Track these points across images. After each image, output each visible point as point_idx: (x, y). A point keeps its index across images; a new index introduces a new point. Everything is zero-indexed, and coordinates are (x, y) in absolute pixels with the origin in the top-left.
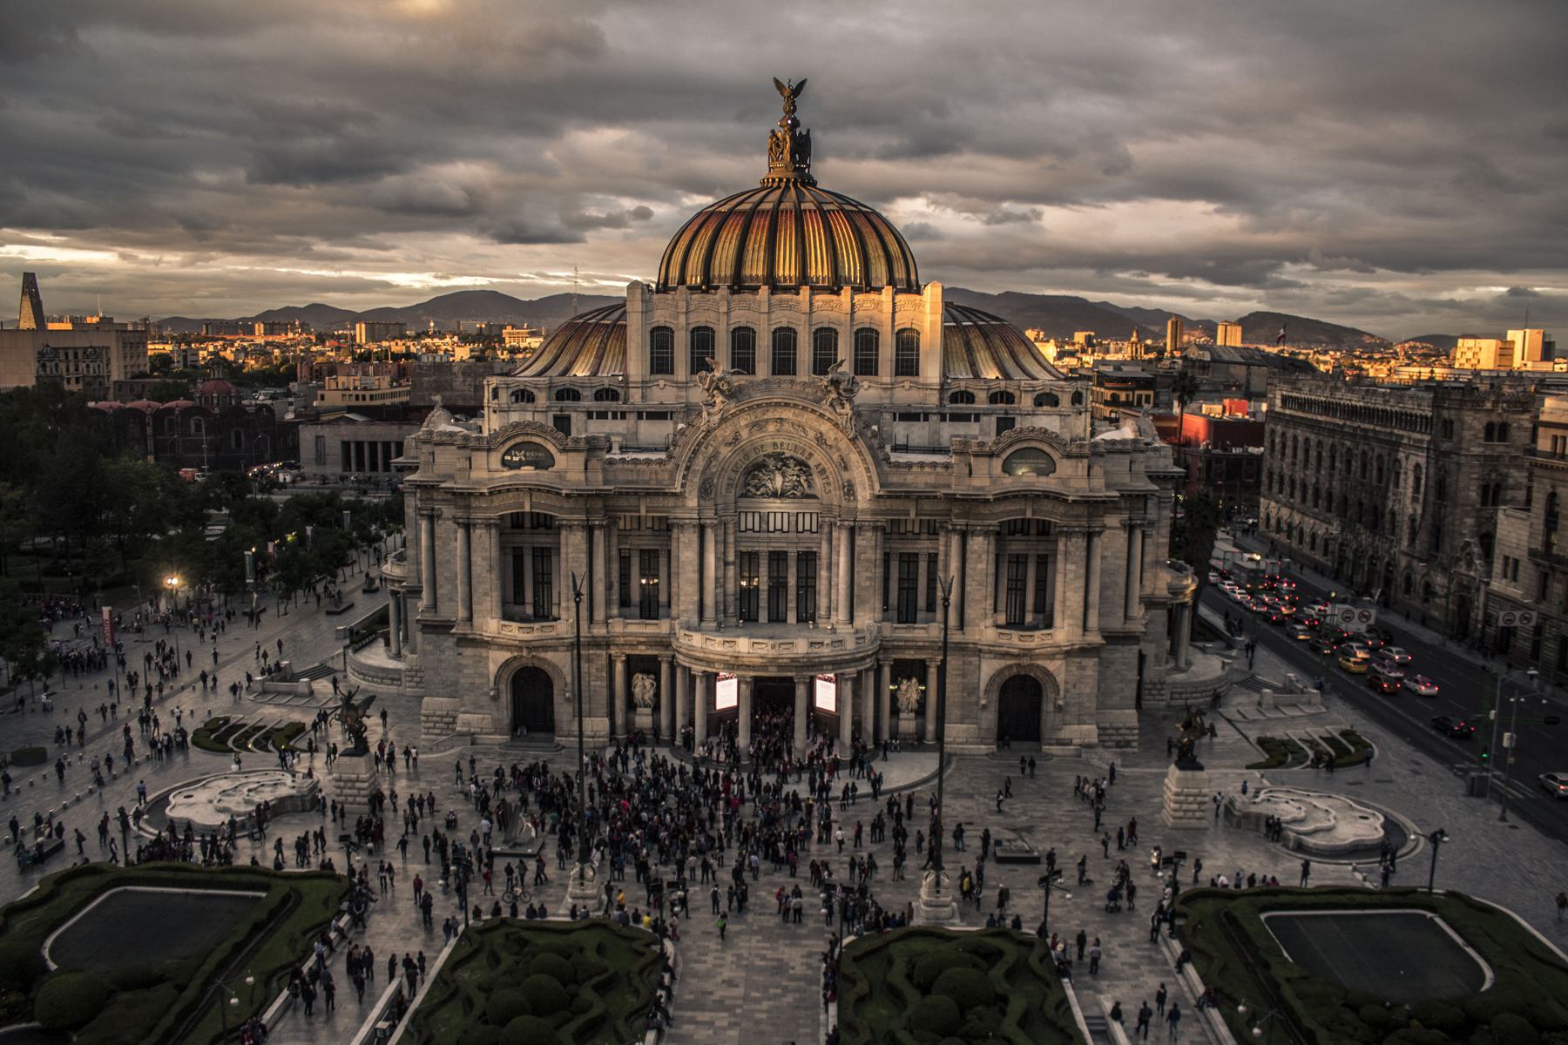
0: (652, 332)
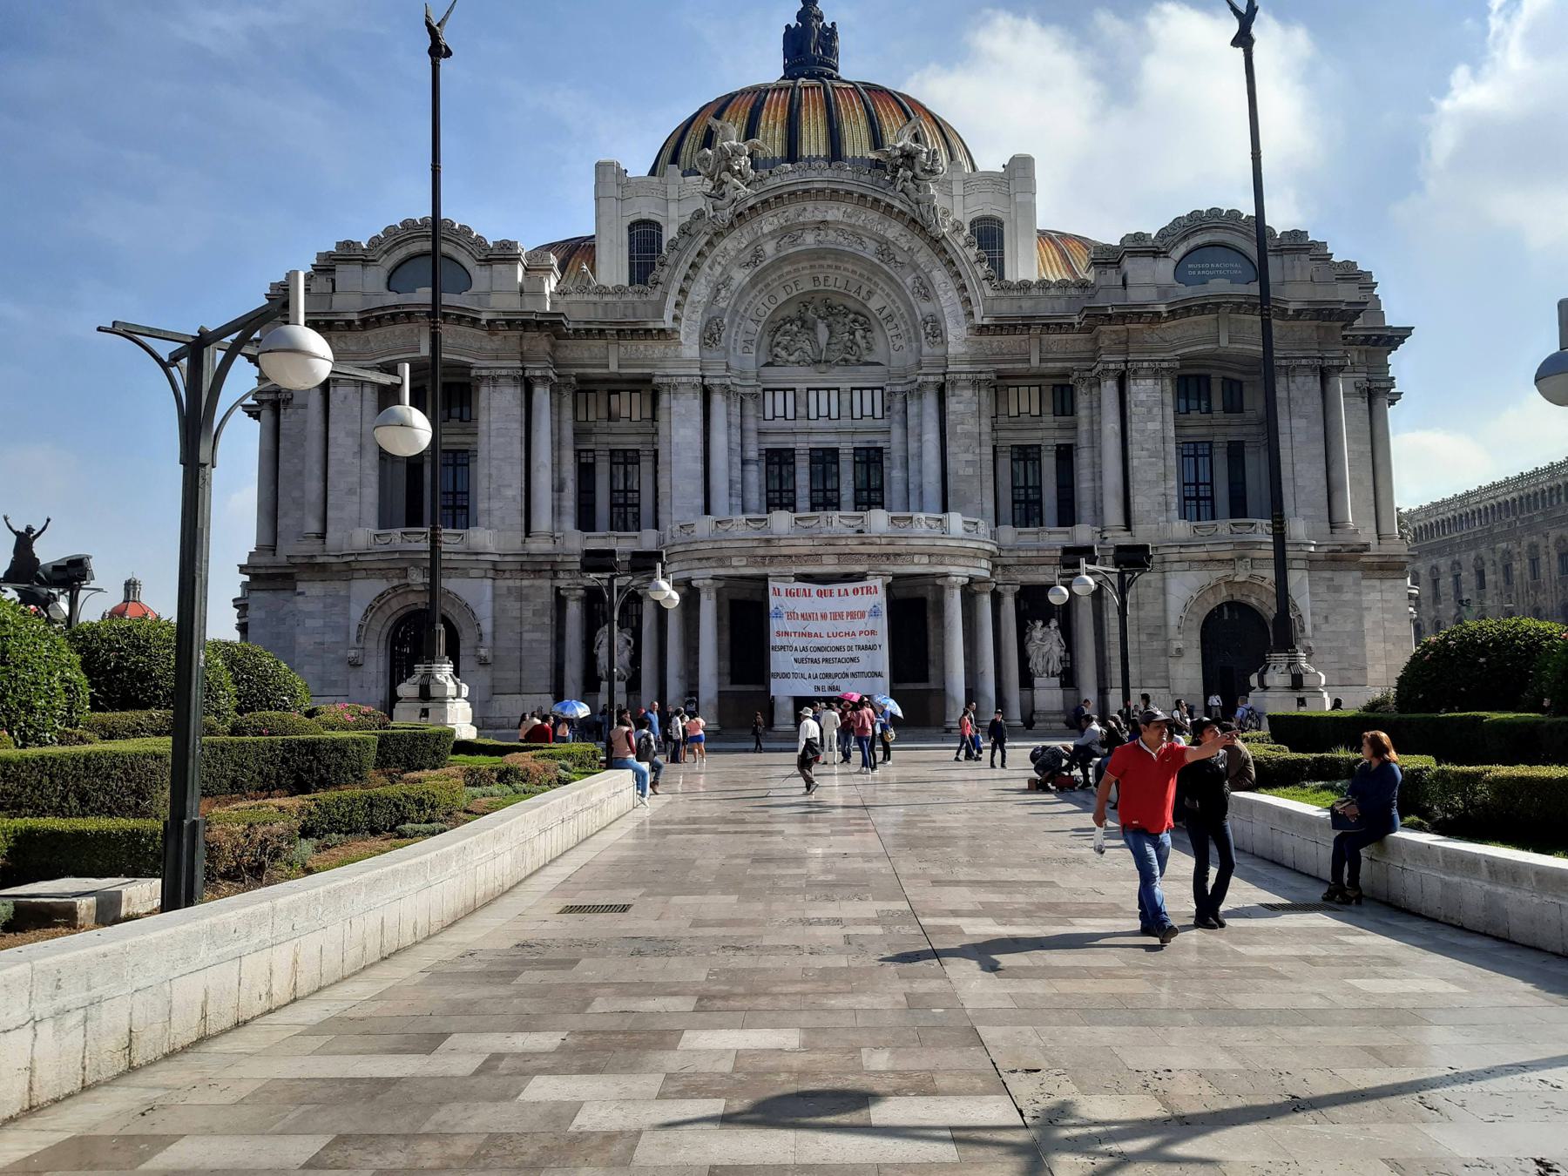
0: (631, 227)
